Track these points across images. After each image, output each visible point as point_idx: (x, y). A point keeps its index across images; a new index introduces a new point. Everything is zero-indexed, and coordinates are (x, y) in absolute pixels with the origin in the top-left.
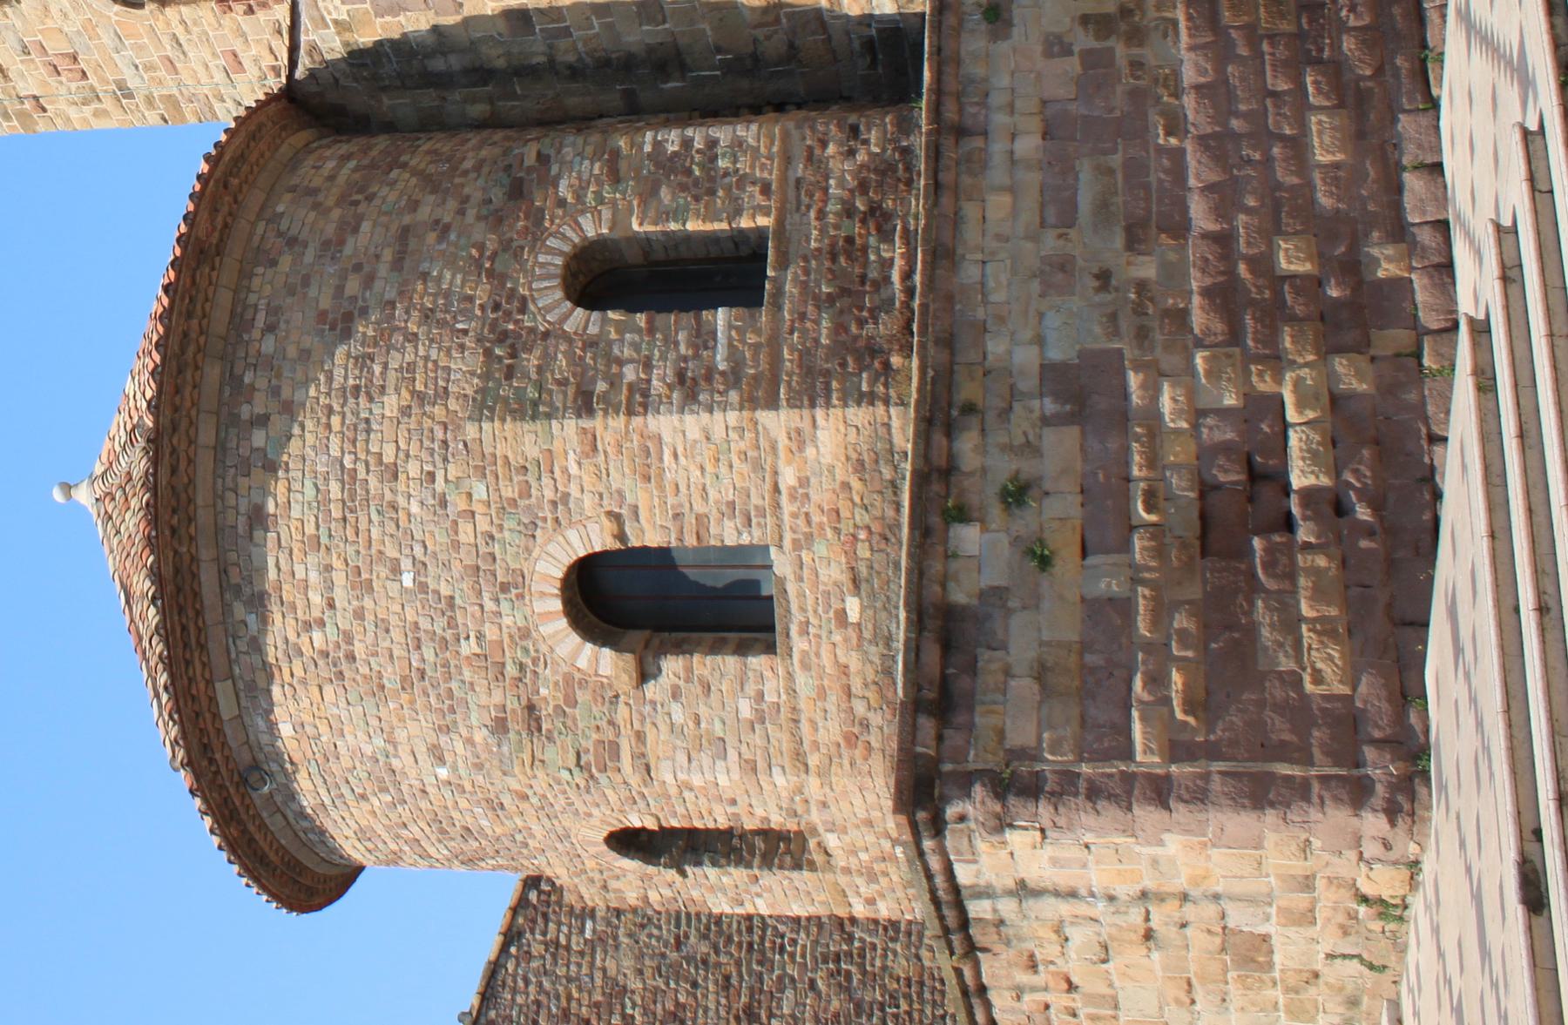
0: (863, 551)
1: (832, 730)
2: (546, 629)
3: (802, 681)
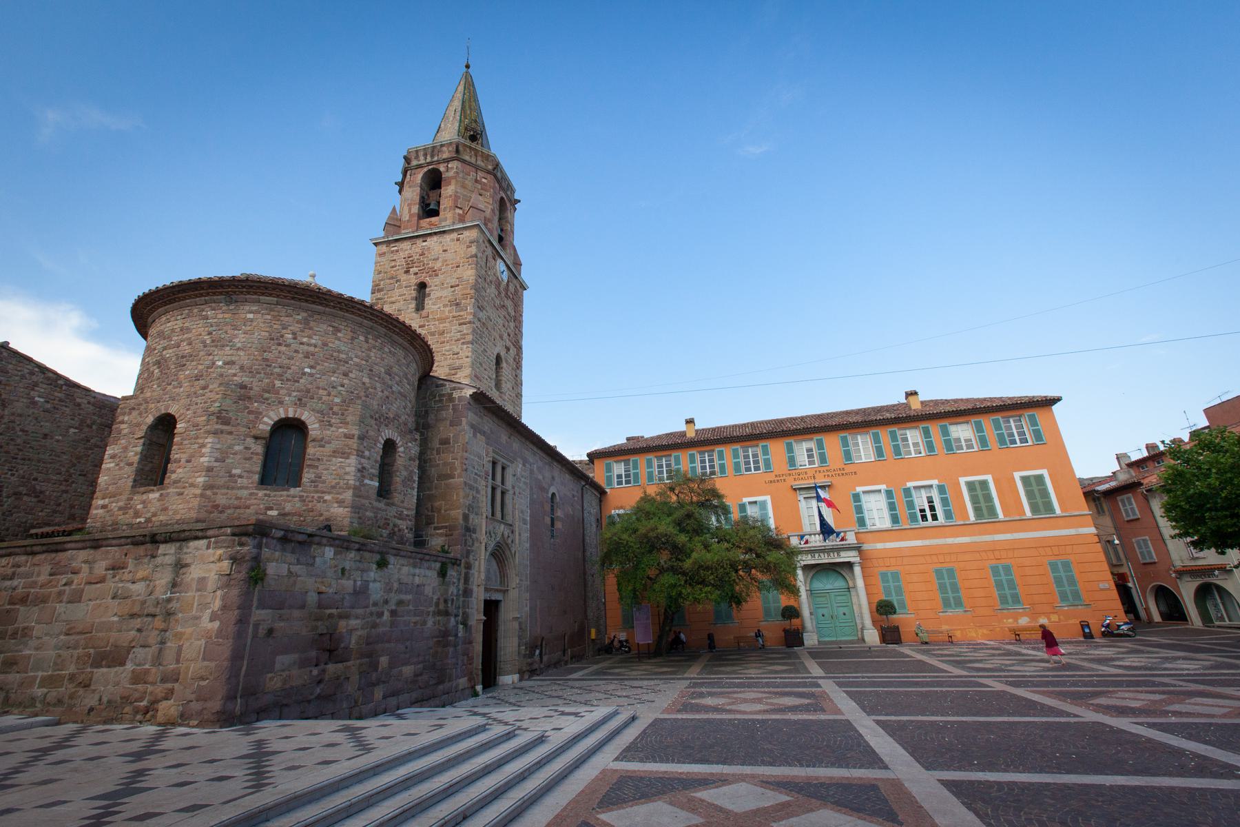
0: (295, 518)
1: (221, 500)
2: (281, 410)
3: (245, 493)
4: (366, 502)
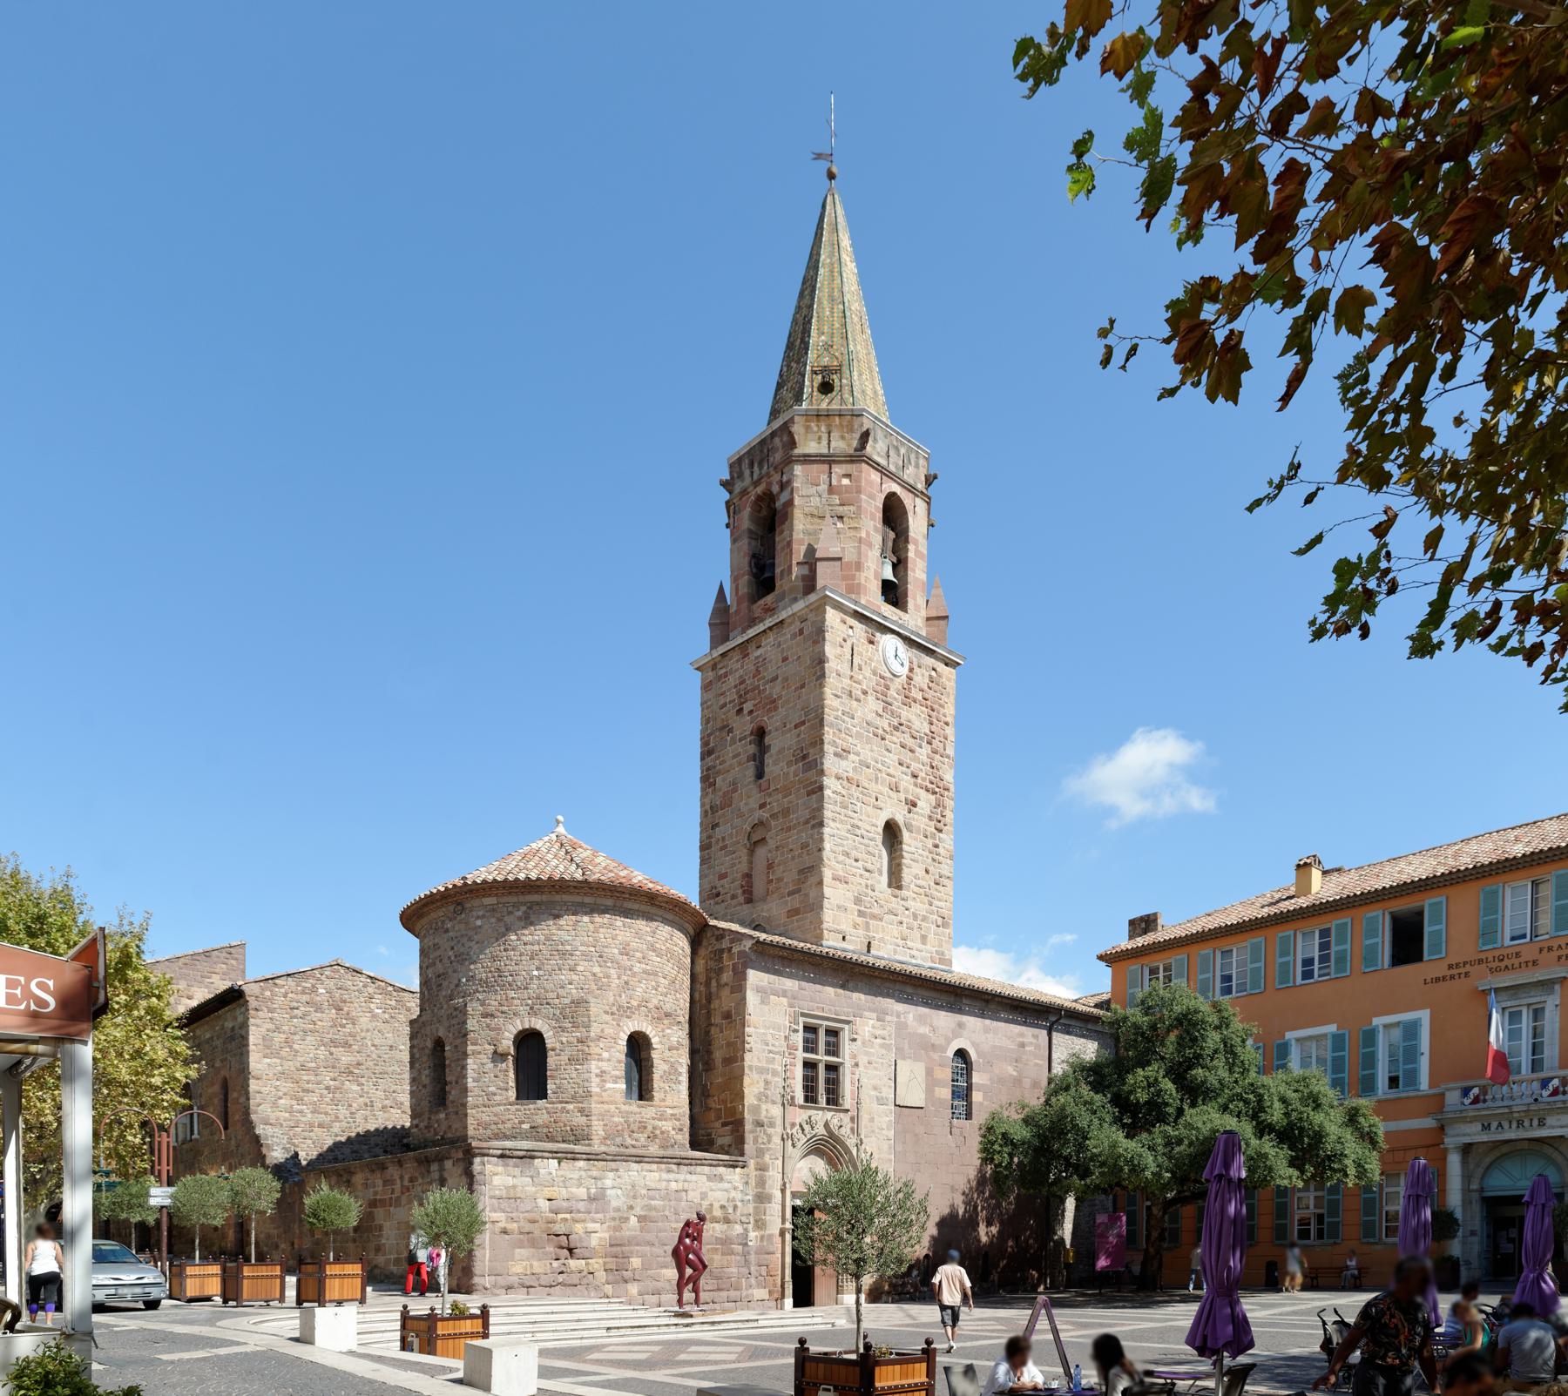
4: (613, 1107)
